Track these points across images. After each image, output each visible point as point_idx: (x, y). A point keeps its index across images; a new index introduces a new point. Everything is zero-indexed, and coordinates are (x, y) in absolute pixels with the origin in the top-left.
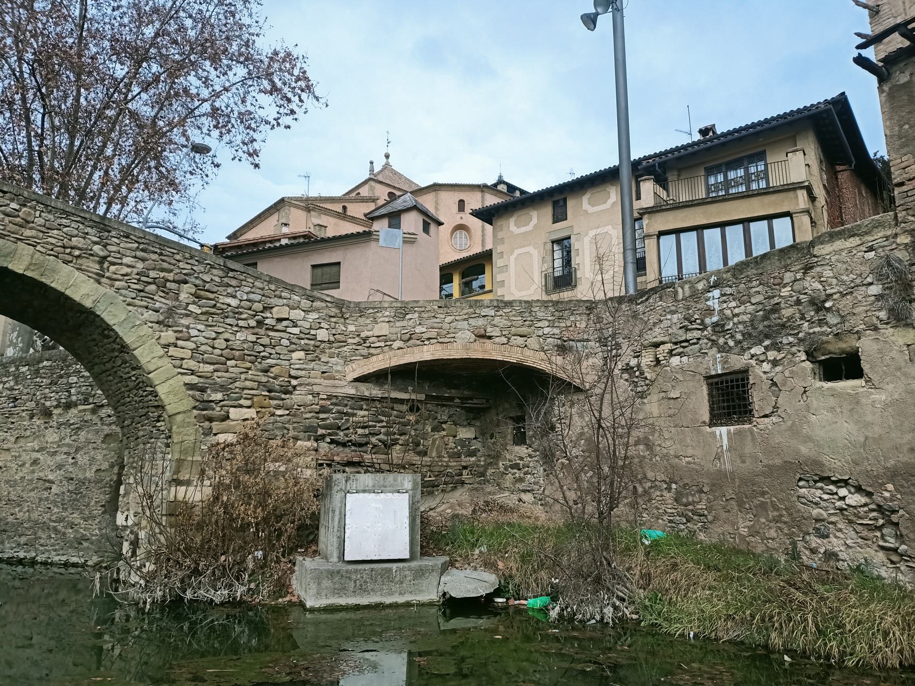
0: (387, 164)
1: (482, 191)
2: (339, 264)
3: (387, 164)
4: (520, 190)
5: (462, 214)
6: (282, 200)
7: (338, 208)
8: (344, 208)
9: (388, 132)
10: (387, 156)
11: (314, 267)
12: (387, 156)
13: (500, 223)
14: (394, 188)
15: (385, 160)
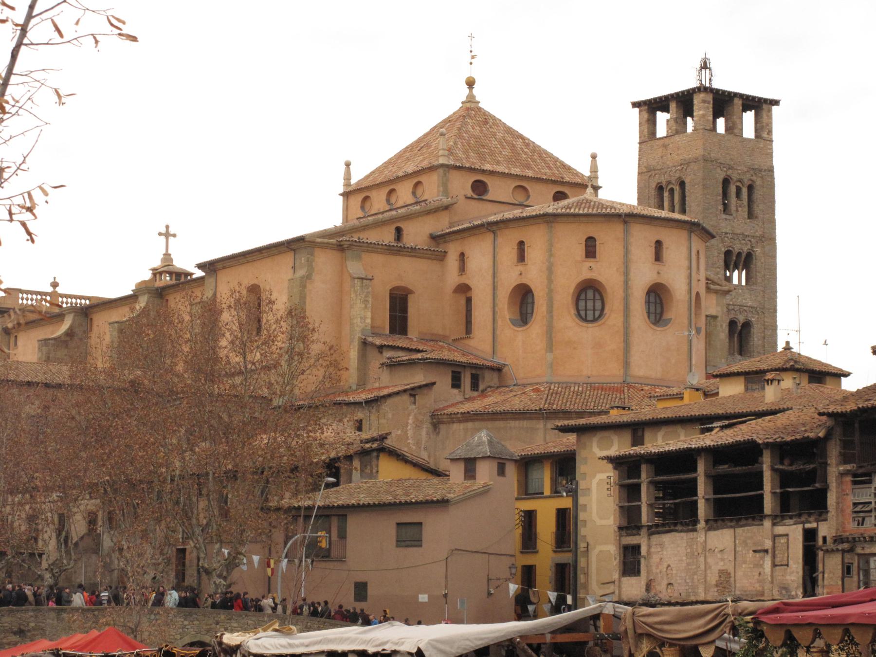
0: (471, 99)
1: (625, 222)
2: (421, 524)
3: (471, 99)
4: (741, 96)
5: (591, 263)
6: (301, 240)
7: (387, 236)
8: (399, 230)
9: (471, 37)
10: (471, 83)
11: (398, 524)
12: (471, 83)
13: (585, 438)
14: (483, 172)
15: (466, 91)
